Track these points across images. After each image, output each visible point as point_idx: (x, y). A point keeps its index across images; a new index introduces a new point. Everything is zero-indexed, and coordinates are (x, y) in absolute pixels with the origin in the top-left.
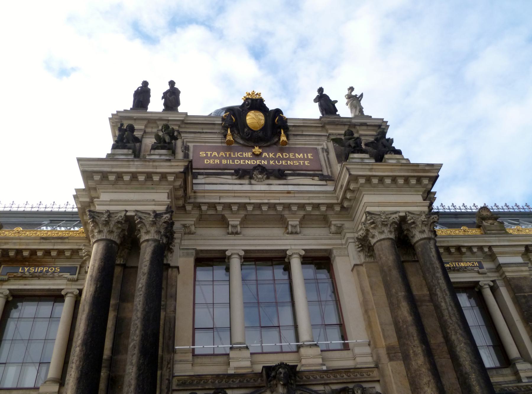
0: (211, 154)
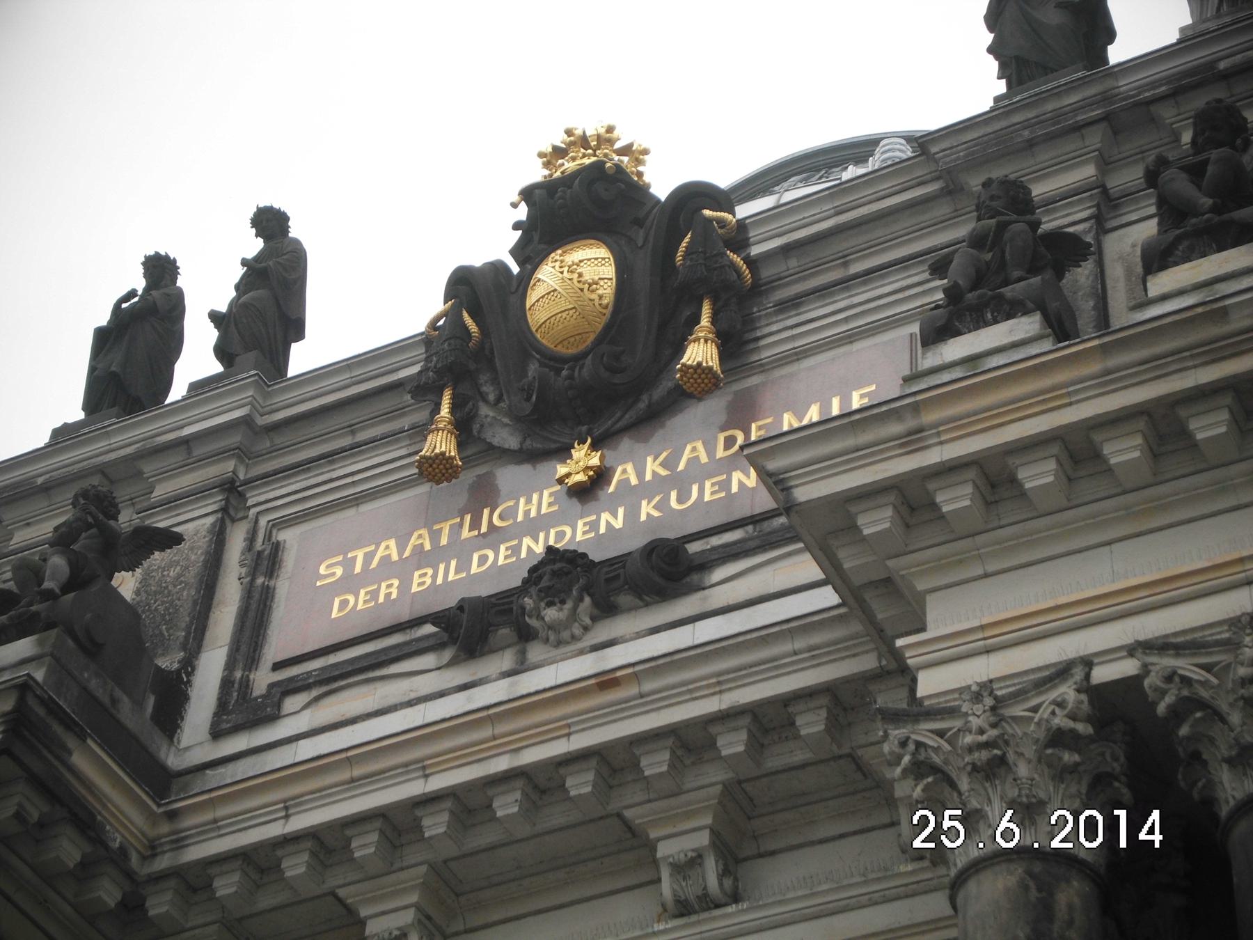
0: (369, 557)
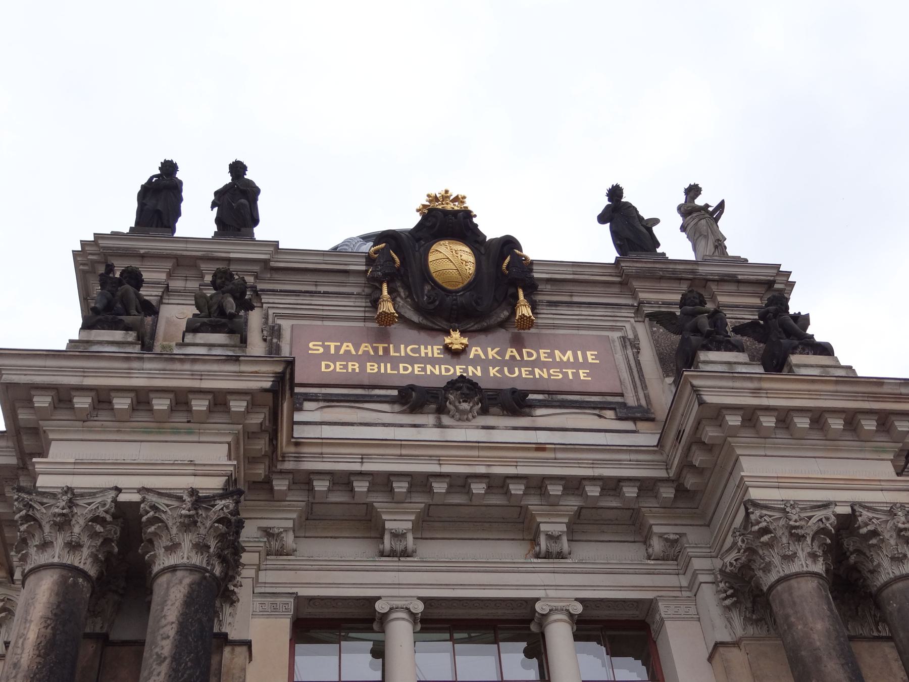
0: (338, 348)
